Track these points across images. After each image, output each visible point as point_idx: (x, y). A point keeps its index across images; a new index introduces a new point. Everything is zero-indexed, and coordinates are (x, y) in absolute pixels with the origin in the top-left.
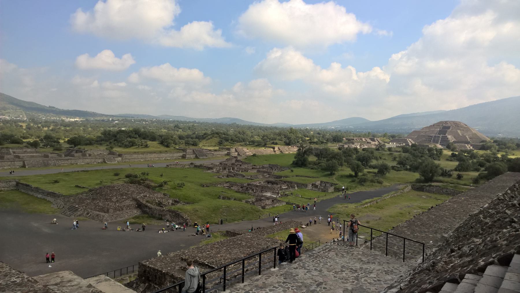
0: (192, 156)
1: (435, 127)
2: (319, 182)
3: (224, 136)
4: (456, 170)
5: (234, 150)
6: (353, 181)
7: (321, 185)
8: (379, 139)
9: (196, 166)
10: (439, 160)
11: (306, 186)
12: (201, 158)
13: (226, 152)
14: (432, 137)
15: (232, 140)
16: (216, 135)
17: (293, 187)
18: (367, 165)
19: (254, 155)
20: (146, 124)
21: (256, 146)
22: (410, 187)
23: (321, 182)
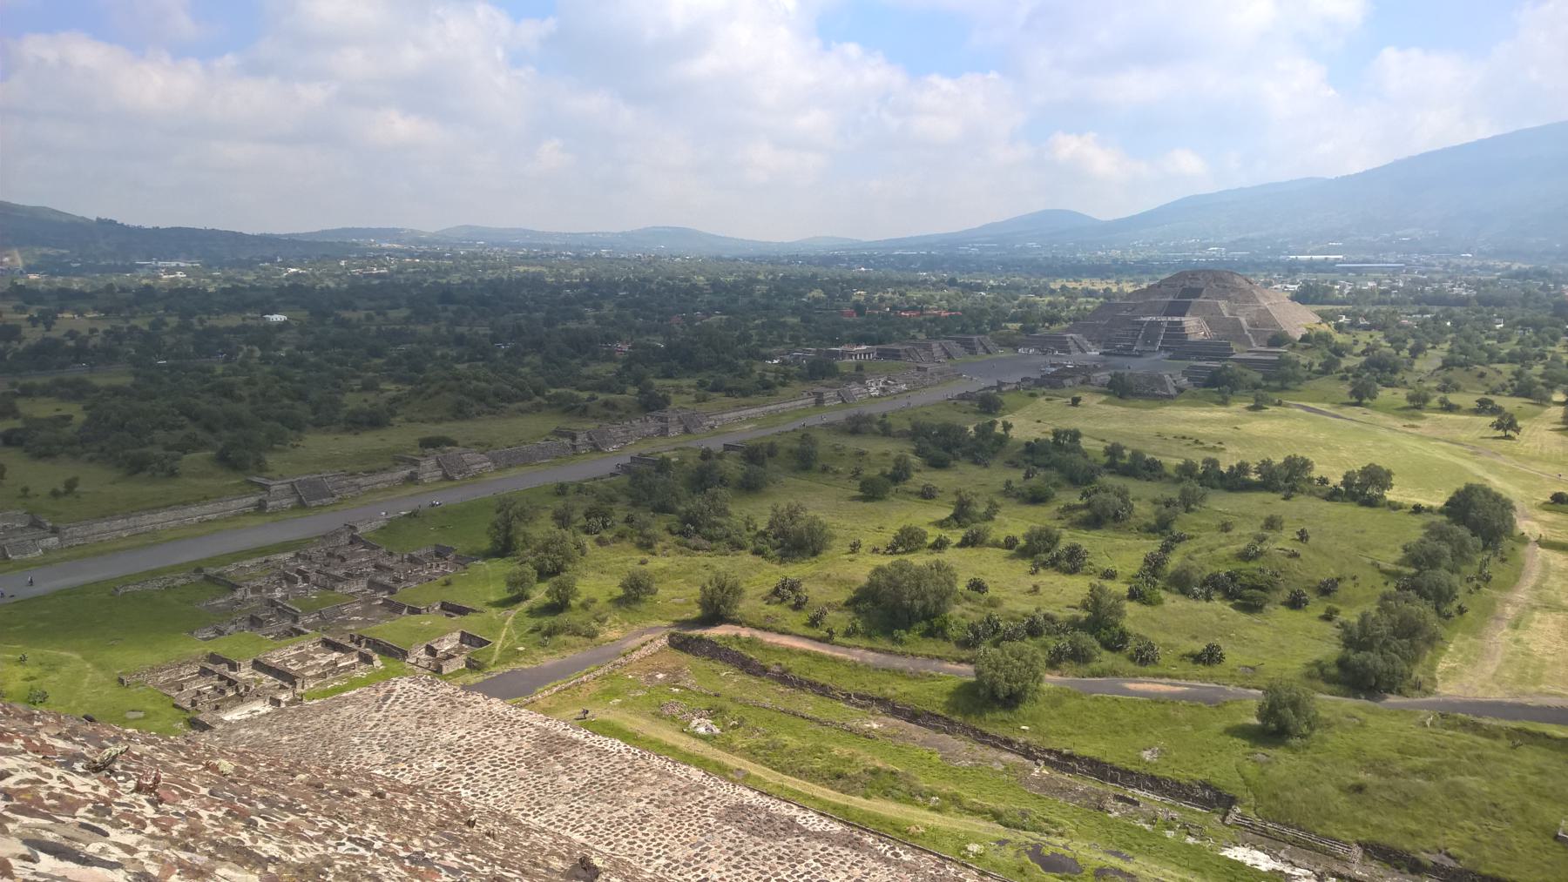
0: (285, 502)
2: (457, 635)
3: (475, 382)
4: (941, 524)
5: (432, 462)
6: (532, 631)
7: (462, 641)
9: (207, 578)
10: (986, 466)
11: (405, 654)
12: (314, 503)
13: (406, 473)
14: (1142, 323)
15: (496, 395)
16: (453, 383)
17: (366, 659)
18: (697, 532)
19: (413, 515)
20: (379, 276)
21: (565, 411)
22: (664, 641)
23: (463, 634)
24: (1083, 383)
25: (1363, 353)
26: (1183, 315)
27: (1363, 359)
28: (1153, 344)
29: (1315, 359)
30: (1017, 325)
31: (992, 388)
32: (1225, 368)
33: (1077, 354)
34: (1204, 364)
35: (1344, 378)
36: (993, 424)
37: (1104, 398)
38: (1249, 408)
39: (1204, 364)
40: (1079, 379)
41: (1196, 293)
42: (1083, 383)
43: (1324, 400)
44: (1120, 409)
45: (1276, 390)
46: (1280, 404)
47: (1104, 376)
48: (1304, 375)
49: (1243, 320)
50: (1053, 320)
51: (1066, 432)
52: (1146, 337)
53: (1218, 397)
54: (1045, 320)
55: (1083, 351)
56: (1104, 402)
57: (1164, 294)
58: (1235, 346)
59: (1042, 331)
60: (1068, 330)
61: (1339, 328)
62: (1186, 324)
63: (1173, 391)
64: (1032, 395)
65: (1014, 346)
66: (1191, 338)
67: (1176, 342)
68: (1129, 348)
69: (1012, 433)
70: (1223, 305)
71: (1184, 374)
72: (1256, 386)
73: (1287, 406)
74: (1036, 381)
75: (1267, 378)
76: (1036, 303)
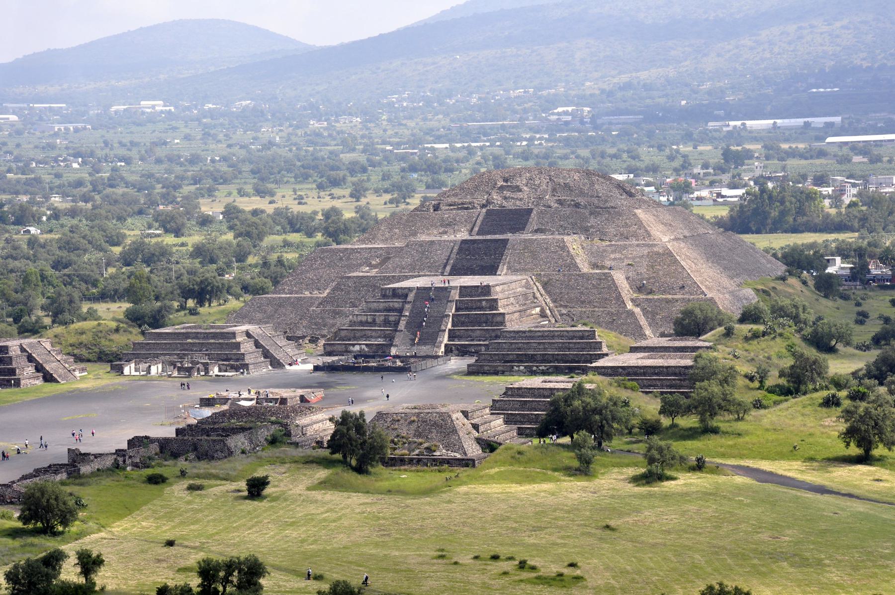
1: (446, 213)
8: (42, 346)
14: (401, 294)
24: (273, 441)
25: (877, 340)
26: (492, 270)
27: (874, 355)
28: (431, 339)
29: (777, 353)
30: (121, 307)
31: (54, 469)
32: (579, 390)
33: (261, 370)
34: (536, 382)
35: (830, 402)
36: (54, 560)
37: (322, 473)
38: (637, 480)
39: (536, 382)
40: (264, 433)
41: (516, 220)
42: (273, 441)
43: (792, 453)
44: (356, 499)
45: (691, 434)
46: (699, 466)
47: (319, 424)
48: (748, 398)
49: (619, 277)
50: (203, 293)
51: (230, 567)
52: (415, 325)
53: (569, 459)
54: (187, 293)
55: (276, 364)
56: (324, 485)
57: (449, 225)
58: (604, 336)
59: (179, 323)
60: (241, 316)
61: (826, 286)
62: (498, 293)
63: (473, 450)
64: (156, 480)
65: (115, 361)
66: (513, 324)
67: (485, 342)
68: (381, 352)
69: (102, 578)
70: (574, 243)
71: (496, 407)
72: (651, 429)
73: (717, 470)
74: (164, 444)
75: (668, 409)
76: (164, 252)
